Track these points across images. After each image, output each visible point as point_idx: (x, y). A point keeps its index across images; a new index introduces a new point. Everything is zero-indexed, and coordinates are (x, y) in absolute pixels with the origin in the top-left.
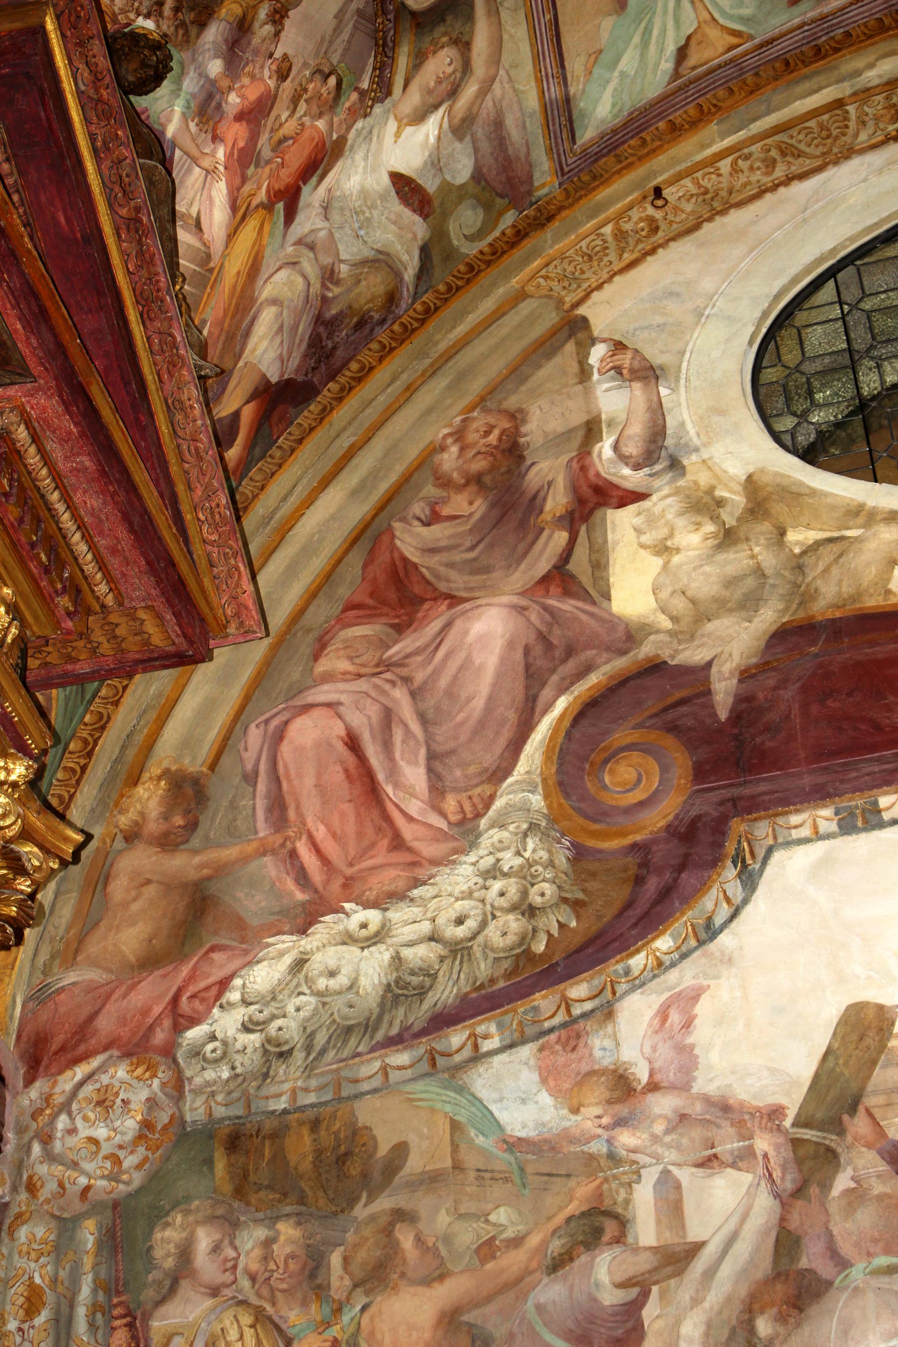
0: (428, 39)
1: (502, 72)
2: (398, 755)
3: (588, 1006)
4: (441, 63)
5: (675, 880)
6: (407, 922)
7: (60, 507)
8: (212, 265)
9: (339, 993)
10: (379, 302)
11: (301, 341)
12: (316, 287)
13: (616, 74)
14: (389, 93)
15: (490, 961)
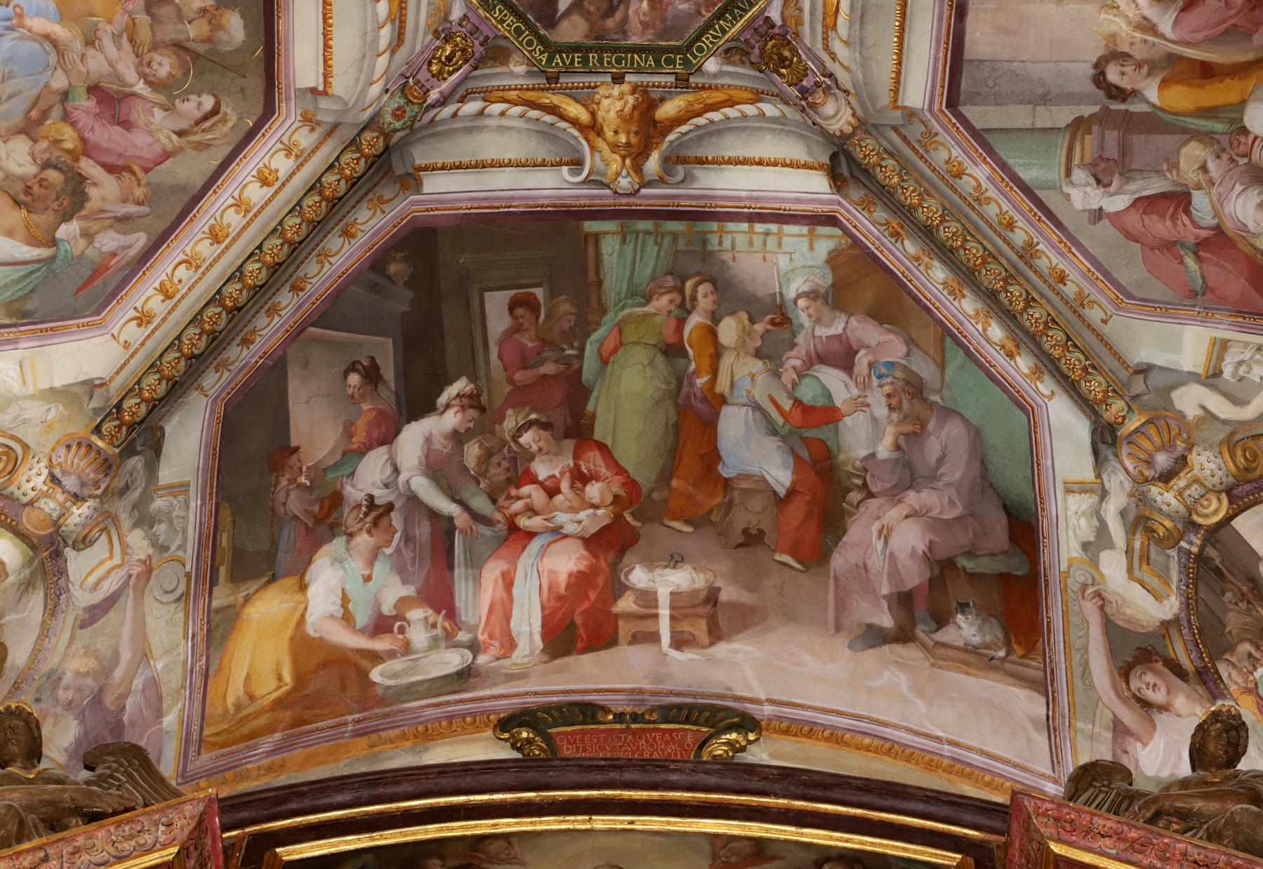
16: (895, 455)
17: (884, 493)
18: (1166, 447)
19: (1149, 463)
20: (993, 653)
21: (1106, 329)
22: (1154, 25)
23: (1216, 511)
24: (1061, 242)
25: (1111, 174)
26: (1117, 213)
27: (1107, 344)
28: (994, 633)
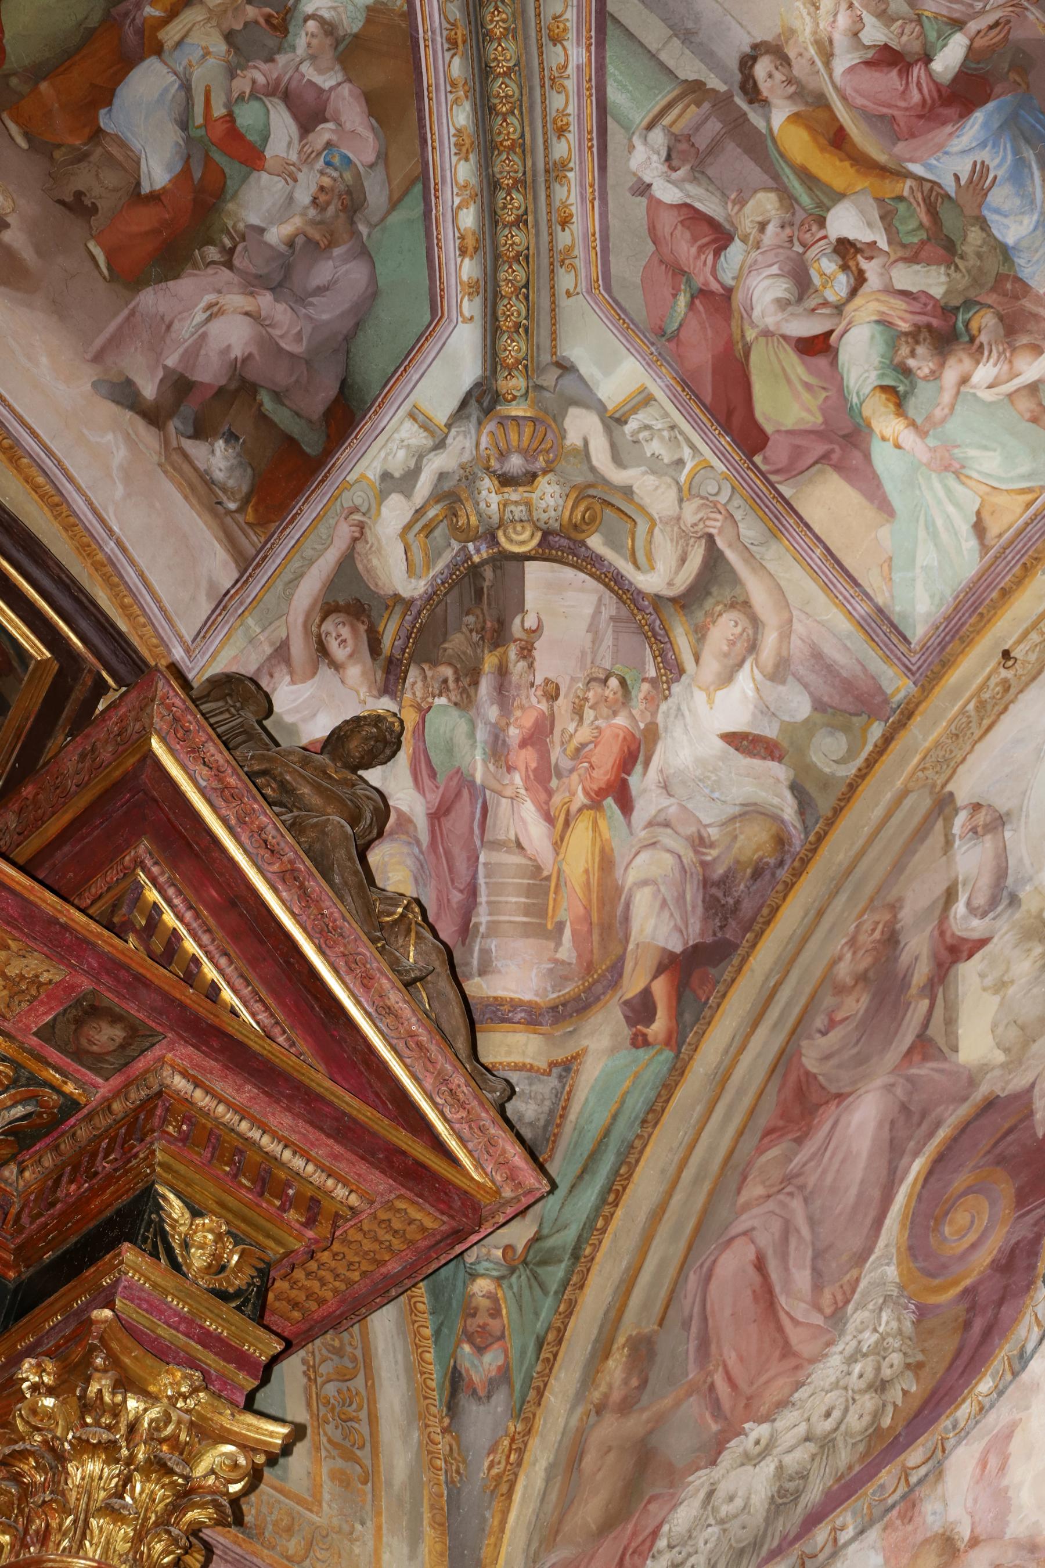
0: (700, 616)
1: (795, 613)
2: (791, 1263)
3: (923, 1471)
4: (726, 628)
5: (996, 1316)
6: (790, 1426)
7: (255, 1134)
8: (545, 873)
9: (735, 1516)
10: (768, 847)
11: (694, 907)
12: (689, 857)
13: (918, 570)
14: (682, 671)
15: (850, 1446)
16: (283, 248)
17: (243, 274)
18: (529, 454)
19: (502, 456)
20: (225, 499)
21: (564, 302)
22: (832, 55)
23: (523, 543)
24: (592, 186)
25: (684, 161)
26: (659, 202)
27: (554, 317)
28: (240, 482)
